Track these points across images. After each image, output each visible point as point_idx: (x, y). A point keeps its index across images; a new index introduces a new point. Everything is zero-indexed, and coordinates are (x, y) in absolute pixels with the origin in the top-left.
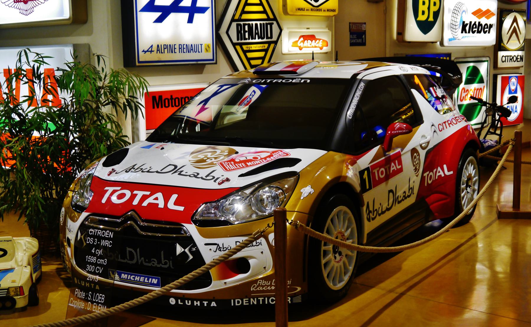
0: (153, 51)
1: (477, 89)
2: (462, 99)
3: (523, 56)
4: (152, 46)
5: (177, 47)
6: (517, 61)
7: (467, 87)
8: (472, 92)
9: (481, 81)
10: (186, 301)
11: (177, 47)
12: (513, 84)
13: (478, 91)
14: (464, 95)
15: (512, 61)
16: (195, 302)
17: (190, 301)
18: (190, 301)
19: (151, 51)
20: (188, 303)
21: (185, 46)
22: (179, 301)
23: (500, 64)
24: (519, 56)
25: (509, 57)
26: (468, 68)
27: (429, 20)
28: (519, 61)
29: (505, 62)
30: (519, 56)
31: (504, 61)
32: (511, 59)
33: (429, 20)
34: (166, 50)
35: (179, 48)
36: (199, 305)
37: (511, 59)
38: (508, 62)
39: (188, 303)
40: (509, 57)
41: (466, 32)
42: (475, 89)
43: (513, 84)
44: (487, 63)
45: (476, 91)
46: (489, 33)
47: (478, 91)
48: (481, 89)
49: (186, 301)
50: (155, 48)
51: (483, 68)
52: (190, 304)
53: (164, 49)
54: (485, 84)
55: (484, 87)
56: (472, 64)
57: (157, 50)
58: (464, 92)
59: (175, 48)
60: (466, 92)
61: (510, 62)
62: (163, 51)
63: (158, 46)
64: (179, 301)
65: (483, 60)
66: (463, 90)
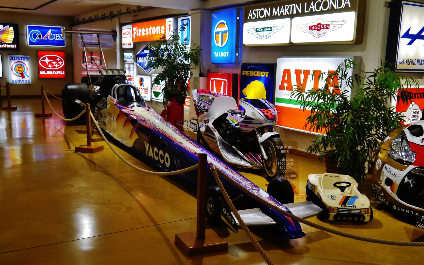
0: (404, 63)
4: (404, 60)
5: (416, 61)
10: (402, 209)
11: (416, 61)
16: (407, 210)
17: (404, 209)
18: (404, 209)
19: (403, 63)
20: (403, 210)
21: (420, 61)
22: (398, 208)
34: (411, 63)
35: (418, 62)
36: (409, 212)
39: (403, 210)
49: (402, 209)
50: (405, 62)
52: (403, 211)
53: (410, 62)
57: (406, 63)
59: (415, 62)
62: (409, 64)
63: (407, 60)
64: (398, 208)
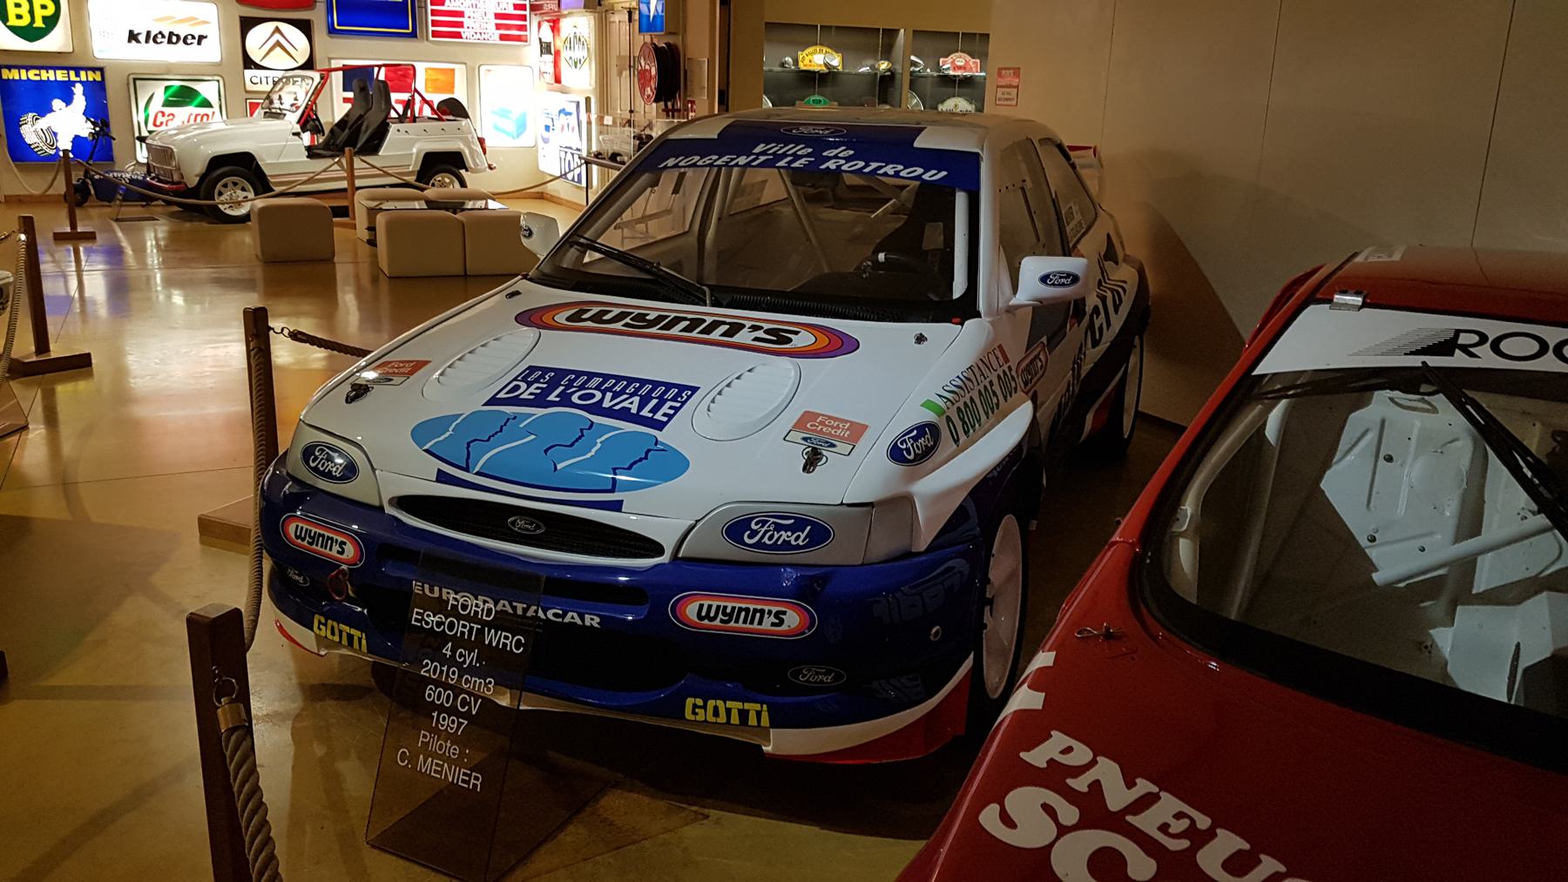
2: (158, 123)
7: (168, 110)
9: (206, 103)
14: (160, 119)
26: (167, 88)
27: (35, 25)
33: (35, 25)
41: (138, 41)
46: (199, 43)
51: (208, 90)
54: (216, 109)
55: (214, 113)
66: (160, 115)
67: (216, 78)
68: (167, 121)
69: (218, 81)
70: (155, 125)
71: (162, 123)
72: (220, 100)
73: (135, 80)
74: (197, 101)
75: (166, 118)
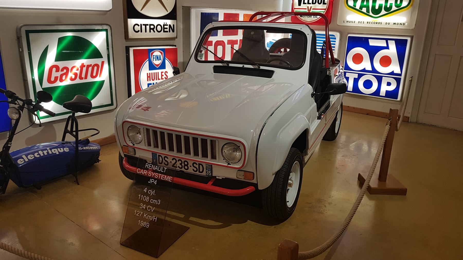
1: (88, 66)
2: (53, 79)
3: (174, 25)
6: (164, 31)
7: (61, 64)
8: (78, 70)
12: (157, 58)
13: (90, 69)
14: (55, 74)
15: (154, 32)
23: (132, 35)
24: (167, 25)
25: (148, 27)
26: (61, 40)
28: (167, 32)
29: (141, 32)
30: (167, 25)
31: (139, 31)
32: (153, 28)
37: (153, 29)
38: (146, 31)
40: (148, 27)
42: (83, 66)
43: (157, 58)
44: (104, 33)
45: (84, 69)
47: (90, 69)
48: (97, 65)
54: (105, 59)
55: (103, 63)
56: (70, 34)
58: (57, 70)
60: (62, 70)
61: (150, 32)
65: (96, 29)
66: (54, 69)
67: (105, 27)
68: (62, 76)
69: (106, 30)
70: (49, 81)
71: (56, 78)
72: (108, 49)
73: (28, 32)
74: (88, 53)
75: (60, 73)
